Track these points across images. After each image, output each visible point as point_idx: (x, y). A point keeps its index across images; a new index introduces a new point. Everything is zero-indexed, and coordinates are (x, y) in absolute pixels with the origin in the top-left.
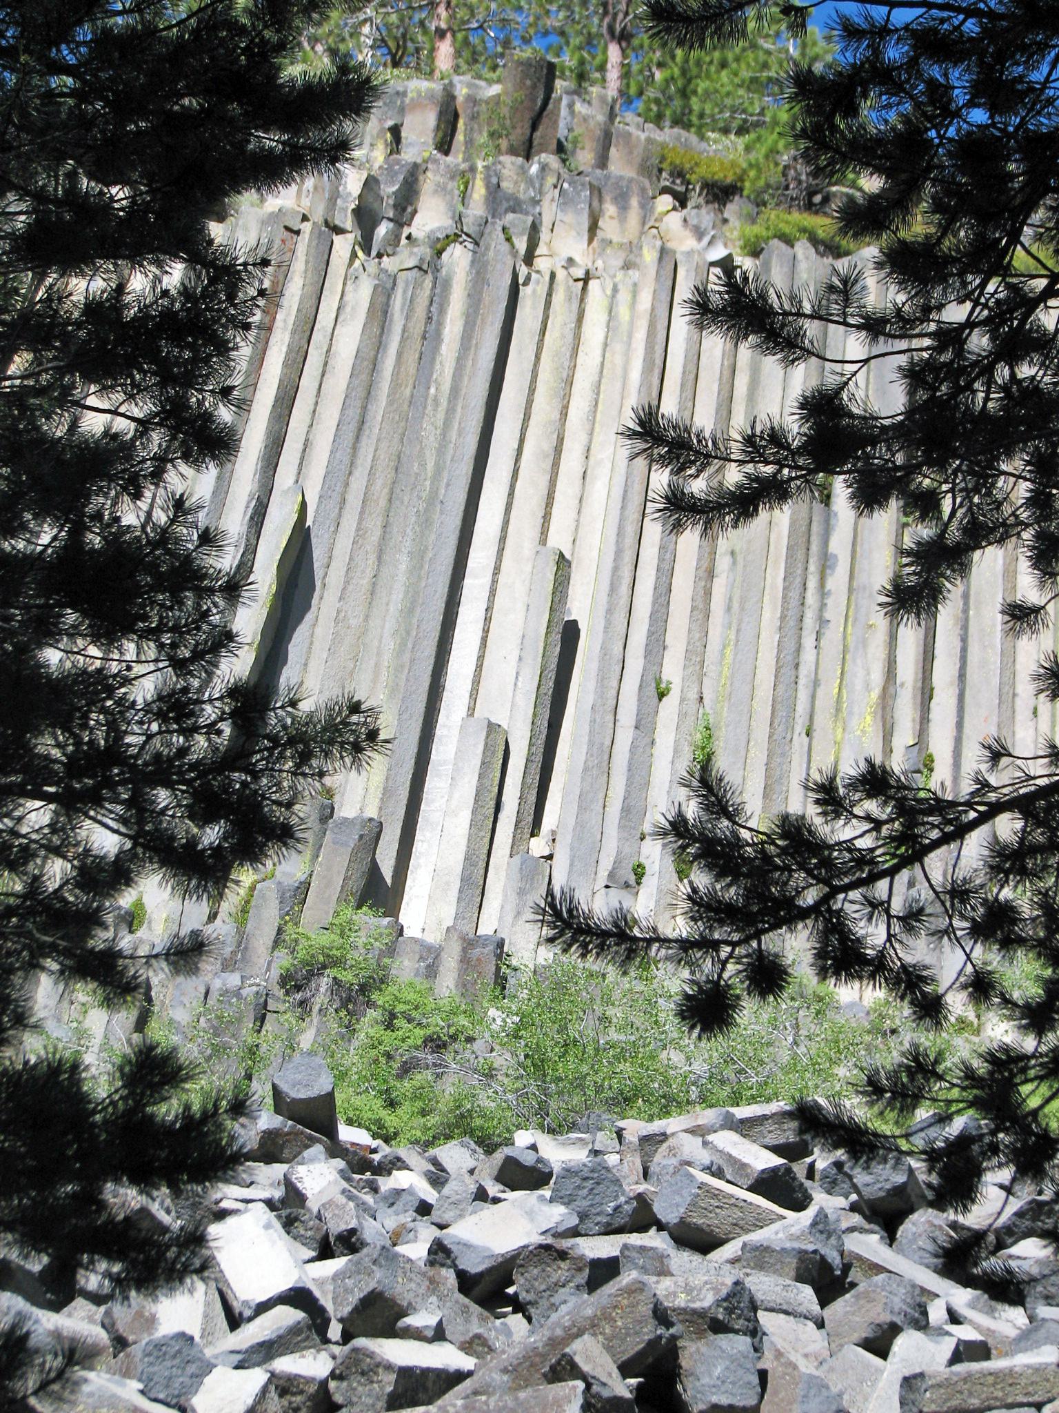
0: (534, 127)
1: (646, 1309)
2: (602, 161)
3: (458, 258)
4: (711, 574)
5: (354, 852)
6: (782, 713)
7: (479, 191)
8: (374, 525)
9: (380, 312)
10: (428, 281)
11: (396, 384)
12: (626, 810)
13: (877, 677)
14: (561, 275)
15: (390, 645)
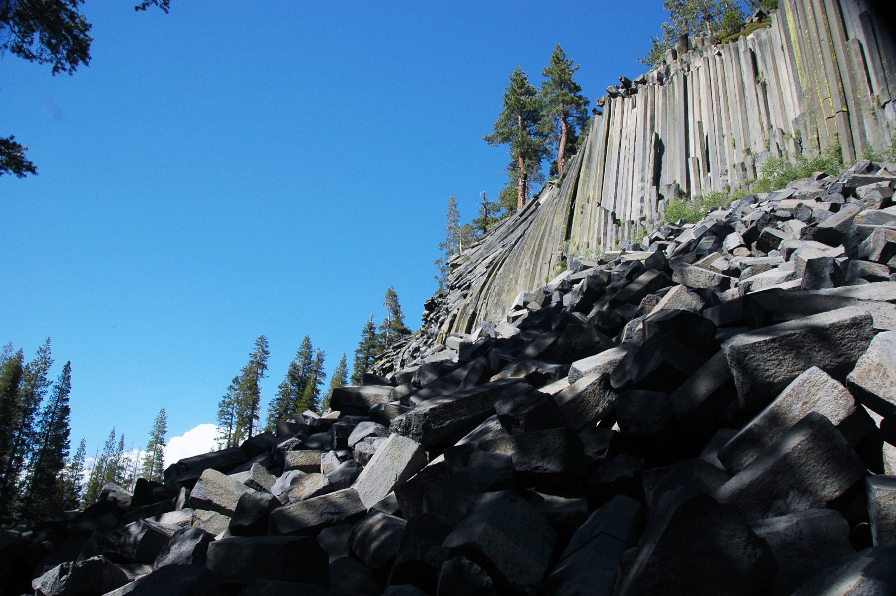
0: (687, 47)
1: (542, 293)
2: (703, 44)
3: (675, 78)
4: (728, 110)
5: (675, 191)
6: (745, 130)
7: (679, 63)
8: (672, 132)
9: (665, 94)
10: (671, 84)
11: (670, 105)
12: (721, 161)
13: (758, 115)
14: (693, 71)
15: (678, 151)
